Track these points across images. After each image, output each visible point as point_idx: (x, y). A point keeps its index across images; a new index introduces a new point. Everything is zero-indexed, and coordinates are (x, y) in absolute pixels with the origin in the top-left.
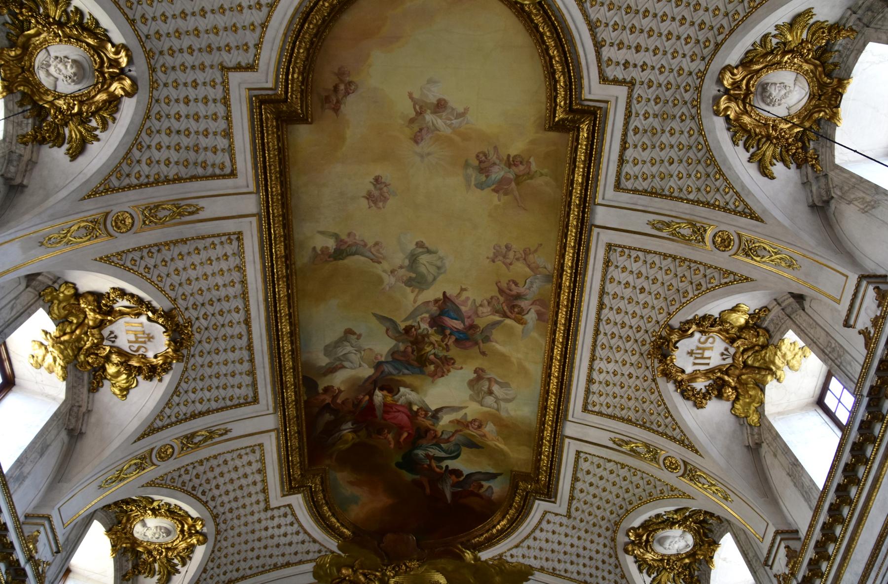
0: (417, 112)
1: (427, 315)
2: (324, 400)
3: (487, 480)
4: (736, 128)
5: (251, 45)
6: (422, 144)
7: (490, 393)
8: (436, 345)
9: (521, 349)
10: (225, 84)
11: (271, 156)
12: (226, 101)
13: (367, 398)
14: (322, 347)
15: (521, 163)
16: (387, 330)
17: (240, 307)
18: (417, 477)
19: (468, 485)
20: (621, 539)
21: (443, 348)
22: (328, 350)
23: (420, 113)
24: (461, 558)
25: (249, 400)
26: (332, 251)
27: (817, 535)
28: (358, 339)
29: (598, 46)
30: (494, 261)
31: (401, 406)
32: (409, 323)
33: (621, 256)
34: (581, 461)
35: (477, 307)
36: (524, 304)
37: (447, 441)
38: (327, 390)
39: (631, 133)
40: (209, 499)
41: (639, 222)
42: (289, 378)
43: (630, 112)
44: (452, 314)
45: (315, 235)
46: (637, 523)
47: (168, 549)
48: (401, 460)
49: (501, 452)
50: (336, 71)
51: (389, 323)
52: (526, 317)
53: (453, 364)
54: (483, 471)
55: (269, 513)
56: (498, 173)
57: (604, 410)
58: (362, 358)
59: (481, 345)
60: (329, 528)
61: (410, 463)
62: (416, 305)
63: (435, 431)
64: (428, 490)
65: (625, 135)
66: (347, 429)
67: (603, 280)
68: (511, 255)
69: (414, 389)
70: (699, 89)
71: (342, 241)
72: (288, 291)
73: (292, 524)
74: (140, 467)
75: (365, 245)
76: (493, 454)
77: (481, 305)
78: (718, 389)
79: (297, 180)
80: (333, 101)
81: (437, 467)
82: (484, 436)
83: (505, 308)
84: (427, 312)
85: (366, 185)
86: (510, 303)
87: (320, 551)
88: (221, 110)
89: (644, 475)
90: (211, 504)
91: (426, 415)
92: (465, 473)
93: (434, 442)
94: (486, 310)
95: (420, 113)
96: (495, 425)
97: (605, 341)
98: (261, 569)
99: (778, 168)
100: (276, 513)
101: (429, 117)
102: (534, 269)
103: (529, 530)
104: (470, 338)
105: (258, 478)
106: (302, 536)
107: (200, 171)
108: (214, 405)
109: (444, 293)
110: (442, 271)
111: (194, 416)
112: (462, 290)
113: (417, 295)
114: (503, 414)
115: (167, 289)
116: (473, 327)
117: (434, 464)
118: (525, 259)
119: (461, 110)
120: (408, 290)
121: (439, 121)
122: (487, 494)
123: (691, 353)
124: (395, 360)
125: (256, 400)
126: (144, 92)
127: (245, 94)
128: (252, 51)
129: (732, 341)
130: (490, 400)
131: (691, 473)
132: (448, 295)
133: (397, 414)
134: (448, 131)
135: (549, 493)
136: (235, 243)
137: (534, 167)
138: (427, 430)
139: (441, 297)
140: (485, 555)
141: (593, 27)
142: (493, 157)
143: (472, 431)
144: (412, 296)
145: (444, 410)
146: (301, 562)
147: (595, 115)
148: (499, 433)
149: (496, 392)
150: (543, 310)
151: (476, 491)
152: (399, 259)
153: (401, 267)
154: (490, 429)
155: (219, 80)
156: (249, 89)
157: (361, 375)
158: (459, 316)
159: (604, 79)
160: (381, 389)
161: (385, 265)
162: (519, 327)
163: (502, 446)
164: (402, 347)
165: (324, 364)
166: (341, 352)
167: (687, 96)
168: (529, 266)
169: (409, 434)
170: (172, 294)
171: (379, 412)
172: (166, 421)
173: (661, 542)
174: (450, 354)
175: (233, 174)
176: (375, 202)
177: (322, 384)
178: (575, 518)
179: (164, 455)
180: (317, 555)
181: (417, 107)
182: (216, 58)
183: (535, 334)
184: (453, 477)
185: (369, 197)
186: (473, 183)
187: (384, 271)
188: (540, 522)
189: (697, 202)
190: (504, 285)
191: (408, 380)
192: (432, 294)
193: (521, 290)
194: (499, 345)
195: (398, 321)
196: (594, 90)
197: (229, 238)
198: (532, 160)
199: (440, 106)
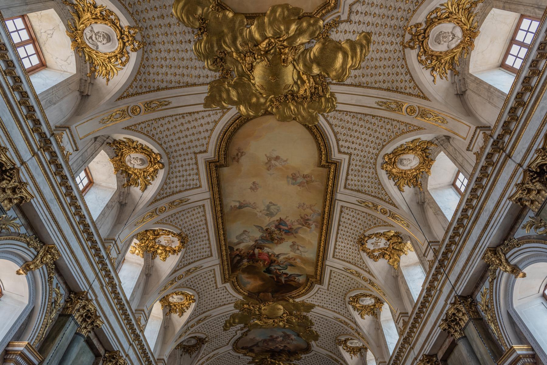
4: (390, 174)
5: (205, 144)
7: (298, 249)
9: (310, 238)
10: (196, 158)
11: (215, 181)
12: (196, 164)
19: (289, 278)
20: (347, 299)
22: (237, 237)
23: (269, 161)
24: (288, 301)
27: (414, 316)
29: (338, 141)
34: (332, 273)
36: (310, 222)
37: (282, 264)
38: (237, 250)
41: (354, 200)
42: (224, 248)
45: (231, 202)
46: (353, 295)
47: (181, 304)
49: (303, 268)
51: (260, 228)
55: (217, 290)
56: (299, 180)
60: (239, 293)
61: (268, 271)
64: (276, 279)
66: (245, 262)
68: (305, 206)
69: (269, 248)
70: (376, 159)
74: (172, 284)
76: (299, 268)
78: (383, 255)
80: (236, 159)
85: (250, 184)
88: (195, 167)
90: (197, 290)
94: (296, 223)
95: (269, 161)
99: (406, 188)
100: (220, 289)
101: (273, 162)
103: (313, 293)
104: (290, 232)
105: (213, 279)
107: (188, 187)
108: (196, 259)
111: (189, 264)
112: (287, 217)
114: (303, 256)
115: (179, 227)
117: (278, 271)
123: (373, 244)
124: (262, 239)
125: (212, 255)
126: (167, 167)
127: (203, 161)
128: (205, 146)
129: (388, 240)
130: (298, 252)
131: (373, 284)
134: (281, 166)
135: (321, 282)
137: (313, 179)
138: (275, 261)
140: (297, 300)
141: (335, 134)
143: (292, 261)
144: (268, 219)
146: (229, 303)
152: (263, 207)
154: (298, 261)
155: (194, 157)
158: (286, 225)
159: (340, 152)
160: (258, 248)
161: (258, 210)
162: (309, 229)
164: (265, 235)
166: (242, 238)
167: (372, 161)
170: (180, 228)
171: (257, 256)
172: (180, 267)
173: (362, 301)
175: (200, 187)
179: (180, 278)
183: (315, 232)
185: (251, 188)
189: (375, 197)
190: (303, 216)
191: (267, 245)
193: (309, 218)
194: (301, 234)
196: (336, 156)
199: (277, 158)
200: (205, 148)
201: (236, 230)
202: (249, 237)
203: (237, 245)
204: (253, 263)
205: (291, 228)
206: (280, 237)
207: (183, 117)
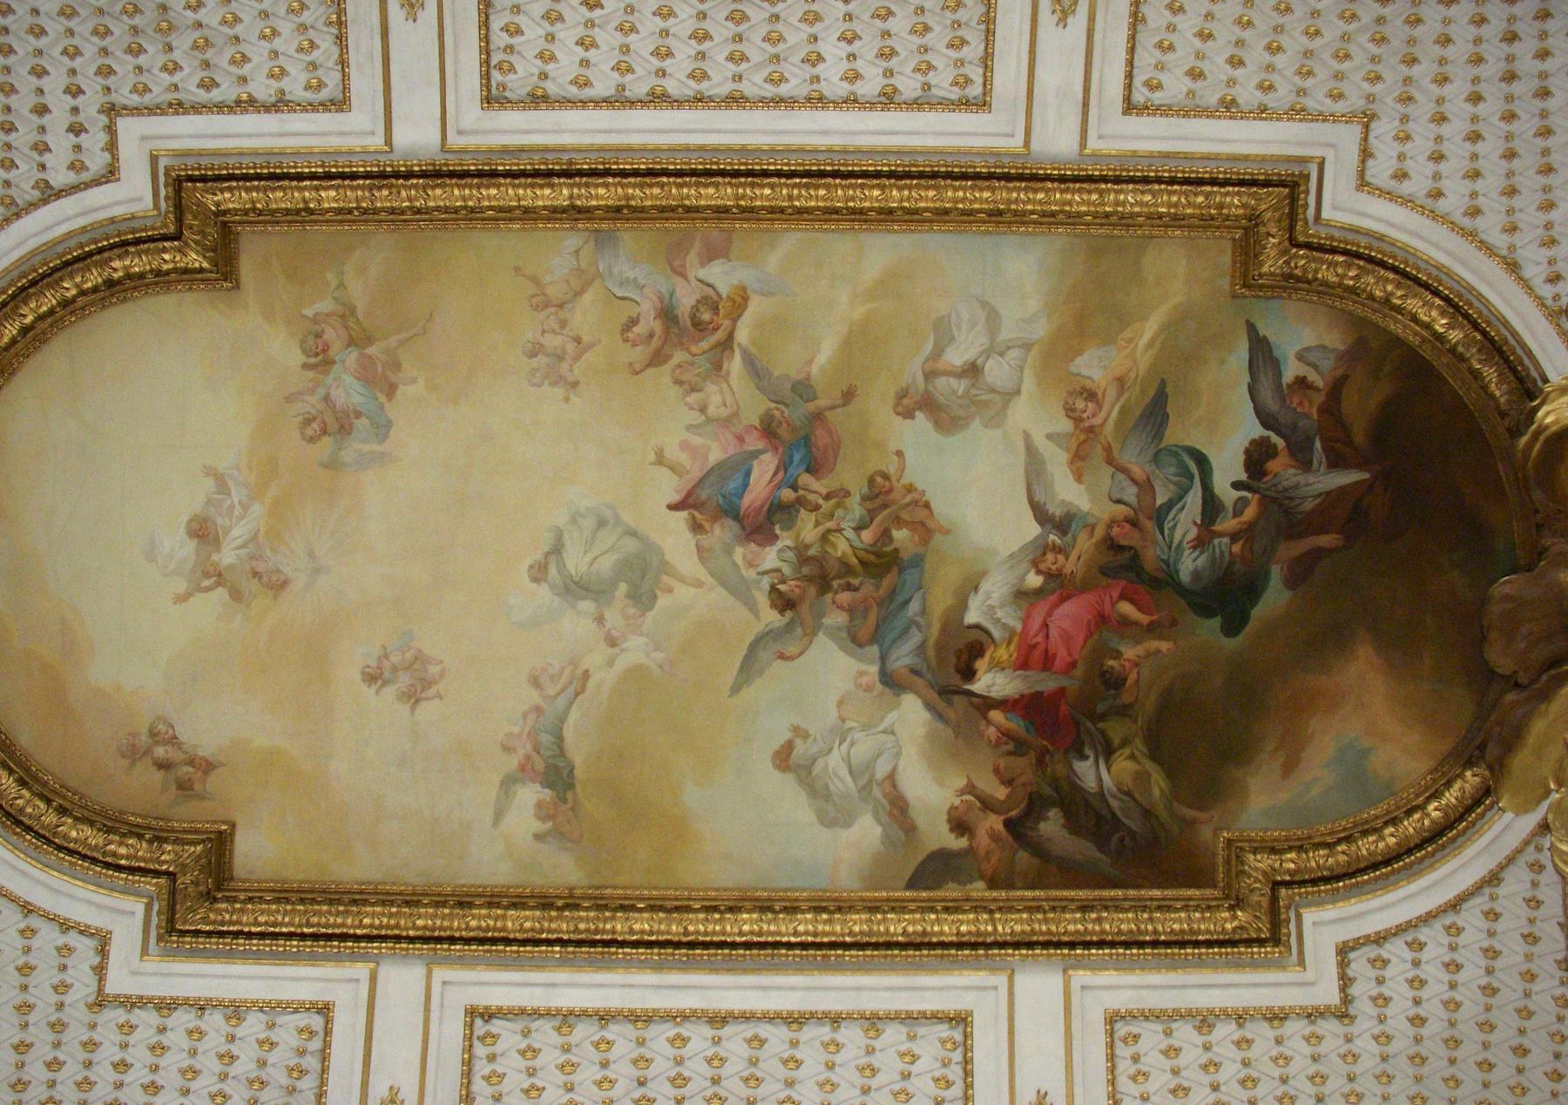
0: (218, 584)
1: (739, 553)
2: (994, 837)
3: (1275, 365)
5: (62, 940)
6: (288, 571)
7: (972, 370)
8: (829, 525)
11: (286, 918)
12: (165, 1006)
13: (996, 715)
14: (824, 835)
15: (318, 336)
16: (782, 656)
17: (671, 1034)
18: (1276, 573)
21: (838, 505)
22: (834, 815)
23: (220, 578)
25: (958, 1037)
26: (547, 794)
28: (805, 735)
30: (575, 384)
32: (763, 600)
33: (512, 69)
35: (709, 420)
36: (686, 299)
37: (1146, 487)
38: (960, 826)
39: (216, 95)
42: (895, 926)
43: (170, 105)
44: (733, 485)
48: (1216, 622)
49: (1172, 327)
50: (126, 763)
52: (724, 289)
53: (886, 477)
54: (1246, 378)
55: (1363, 1007)
56: (348, 389)
57: (974, 50)
58: (865, 727)
59: (823, 402)
60: (1439, 838)
61: (1227, 596)
62: (709, 580)
63: (1112, 522)
64: (1325, 540)
65: (220, 108)
67: (583, 104)
68: (552, 342)
71: (522, 768)
72: (641, 910)
75: (538, 710)
77: (703, 410)
80: (188, 772)
82: (1120, 381)
83: (705, 345)
84: (729, 552)
86: (692, 334)
87: (1537, 867)
88: (182, 1019)
91: (1057, 550)
92: (1258, 431)
93: (1149, 525)
94: (714, 395)
95: (220, 578)
96: (1080, 353)
97: (758, 78)
100: (1362, 989)
101: (227, 556)
102: (584, 280)
103: (1441, 233)
104: (802, 435)
109: (673, 507)
110: (608, 514)
112: (660, 460)
113: (682, 580)
114: (1041, 330)
116: (768, 430)
117: (1227, 524)
118: (561, 306)
119: (210, 483)
120: (663, 601)
121: (235, 532)
122: (1328, 364)
124: (875, 638)
127: (153, 964)
128: (73, 938)
130: (997, 372)
132: (676, 498)
133: (1053, 632)
134: (257, 509)
136: (497, 1026)
137: (326, 306)
139: (684, 514)
142: (312, 404)
143: (1109, 417)
144: (683, 593)
145: (1040, 497)
147: (184, 183)
148: (1108, 340)
149: (969, 356)
150: (698, 245)
151: (1320, 398)
152: (576, 625)
153: (600, 620)
154: (1093, 366)
155: (120, 1015)
156: (145, 951)
157: (921, 731)
158: (741, 466)
159: (111, 174)
160: (969, 674)
161: (594, 659)
164: (837, 619)
165: (878, 830)
168: (579, 294)
169: (1122, 597)
171: (1047, 683)
174: (858, 488)
175: (325, 1009)
176: (427, 683)
177: (941, 836)
178: (1371, 99)
181: (206, 583)
182: (77, 1014)
183: (773, 261)
184: (1273, 465)
185: (413, 697)
186: (376, 447)
187: (610, 663)
188: (1407, 201)
190: (639, 354)
191: (940, 602)
192: (675, 539)
195: (760, 627)
196: (133, 195)
197: (482, 1039)
198: (309, 312)
199: (203, 532)
200: (85, 948)
201: (756, 823)
202: (841, 734)
203: (910, 829)
204: (1124, 711)
205: (768, 430)
206: (856, 508)
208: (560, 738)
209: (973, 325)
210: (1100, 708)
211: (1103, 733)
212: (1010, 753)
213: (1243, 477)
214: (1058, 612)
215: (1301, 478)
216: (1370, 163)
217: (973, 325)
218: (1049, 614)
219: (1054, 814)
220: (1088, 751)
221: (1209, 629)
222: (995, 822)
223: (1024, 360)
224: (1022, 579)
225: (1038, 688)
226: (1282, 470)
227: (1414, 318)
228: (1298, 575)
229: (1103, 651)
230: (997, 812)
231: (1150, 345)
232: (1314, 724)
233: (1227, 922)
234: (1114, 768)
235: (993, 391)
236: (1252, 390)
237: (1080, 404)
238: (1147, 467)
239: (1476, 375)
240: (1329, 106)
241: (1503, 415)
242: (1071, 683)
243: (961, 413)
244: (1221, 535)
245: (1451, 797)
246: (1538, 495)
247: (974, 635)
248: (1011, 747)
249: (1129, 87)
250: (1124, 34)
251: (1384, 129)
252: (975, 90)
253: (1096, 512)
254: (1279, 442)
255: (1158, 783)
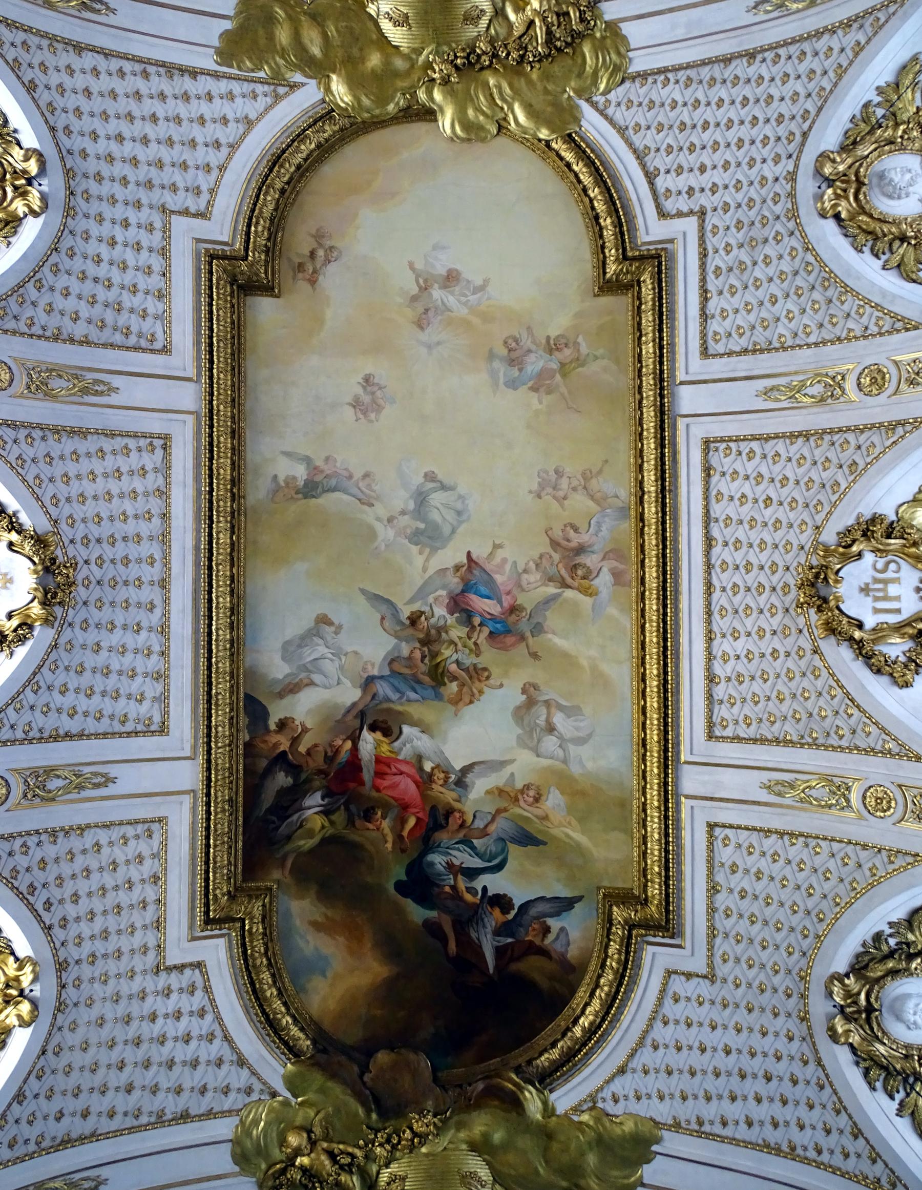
0: (420, 287)
1: (444, 593)
2: (276, 745)
3: (557, 914)
5: (204, 188)
6: (428, 330)
8: (460, 646)
9: (595, 638)
10: (166, 230)
12: (164, 252)
13: (349, 745)
14: (278, 645)
15: (566, 345)
16: (383, 618)
17: (156, 556)
18: (433, 914)
19: (522, 925)
20: (820, 1008)
21: (471, 650)
22: (290, 650)
23: (425, 289)
25: (153, 728)
26: (301, 483)
28: (336, 633)
30: (539, 497)
31: (405, 762)
32: (416, 607)
33: (726, 456)
35: (519, 575)
37: (484, 833)
38: (283, 725)
39: (711, 276)
40: (55, 921)
42: (221, 687)
43: (705, 249)
44: (483, 590)
45: (277, 457)
48: (404, 877)
49: (578, 849)
50: (314, 232)
52: (596, 582)
53: (488, 678)
55: (163, 980)
56: (535, 363)
57: (742, 732)
58: (341, 668)
59: (531, 640)
60: (270, 1026)
61: (420, 884)
62: (427, 575)
64: (452, 946)
65: (703, 280)
67: (706, 498)
68: (564, 483)
71: (316, 468)
72: (231, 538)
73: (202, 1013)
75: (350, 477)
77: (525, 571)
79: (257, 372)
80: (309, 270)
81: (469, 890)
82: (546, 818)
83: (563, 572)
84: (444, 587)
85: (352, 387)
86: (570, 564)
87: (249, 1091)
89: (836, 846)
91: (447, 778)
92: (517, 903)
93: (461, 835)
94: (534, 577)
95: (425, 289)
96: (562, 793)
97: (724, 602)
98: (130, 1122)
100: (174, 980)
101: (437, 293)
102: (600, 500)
106: (218, 1047)
107: (118, 338)
109: (469, 553)
110: (465, 517)
112: (496, 547)
113: (427, 560)
114: (575, 770)
116: (514, 609)
117: (462, 883)
118: (585, 488)
119: (479, 282)
120: (415, 549)
121: (451, 298)
122: (559, 947)
126: (55, 216)
128: (205, 196)
130: (550, 743)
132: (474, 556)
134: (464, 312)
136: (159, 453)
137: (584, 349)
138: (449, 812)
139: (465, 561)
141: (640, 156)
142: (527, 343)
143: (523, 810)
144: (419, 561)
145: (477, 769)
146: (210, 1115)
147: (659, 261)
148: (570, 810)
150: (622, 567)
151: (537, 942)
152: (401, 500)
153: (403, 513)
155: (158, 224)
156: (198, 241)
157: (339, 700)
158: (493, 594)
160: (373, 728)
161: (380, 510)
162: (587, 601)
163: (577, 836)
164: (405, 650)
165: (280, 676)
166: (309, 655)
168: (592, 498)
169: (418, 819)
171: (367, 775)
174: (482, 661)
176: (365, 413)
177: (277, 712)
180: (242, 1099)
181: (421, 281)
182: (156, 196)
183: (613, 611)
184: (497, 912)
185: (356, 404)
186: (502, 381)
187: (378, 519)
190: (557, 534)
192: (451, 555)
193: (584, 538)
194: (558, 639)
195: (400, 605)
196: (650, 229)
197: (151, 444)
198: (580, 339)
199: (451, 278)
202: (338, 653)
203: (281, 695)
204: (351, 822)
205: (514, 609)
206: (469, 660)
207: (146, 75)
208: (333, 490)
209: (577, 729)
210: (353, 808)
211: (338, 809)
212: (326, 753)
213: (490, 893)
214: (409, 781)
215: (489, 930)
216: (683, 978)
217: (577, 729)
218: (408, 776)
219: (290, 780)
220: (326, 800)
221: (399, 873)
222: (285, 745)
223: (557, 759)
224: (429, 759)
225: (365, 770)
226: (496, 917)
227: (587, 1004)
228: (432, 928)
229: (386, 808)
230: (291, 745)
231: (567, 835)
232: (341, 939)
233: (220, 889)
234: (317, 816)
235: (539, 741)
236: (542, 899)
237: (532, 793)
238: (494, 836)
239: (554, 1045)
240: (718, 953)
241: (529, 1062)
242: (367, 789)
243: (526, 722)
244: (455, 880)
245: (295, 1031)
246: (480, 1086)
247: (396, 731)
248: (330, 754)
249: (724, 826)
250: (758, 825)
251: (704, 988)
252: (718, 733)
253: (468, 803)
254: (510, 916)
255: (307, 844)
